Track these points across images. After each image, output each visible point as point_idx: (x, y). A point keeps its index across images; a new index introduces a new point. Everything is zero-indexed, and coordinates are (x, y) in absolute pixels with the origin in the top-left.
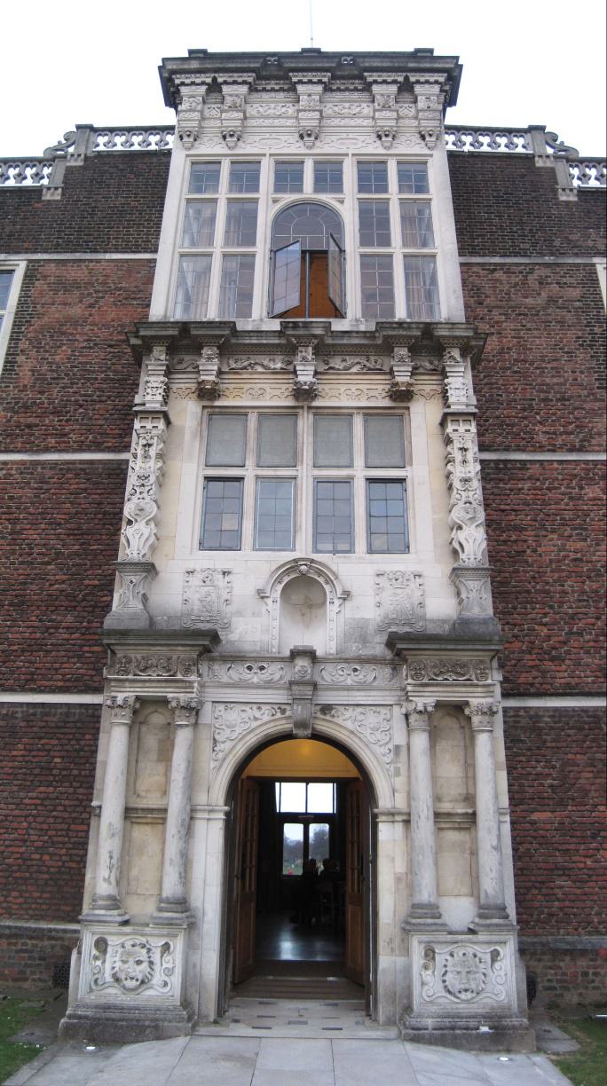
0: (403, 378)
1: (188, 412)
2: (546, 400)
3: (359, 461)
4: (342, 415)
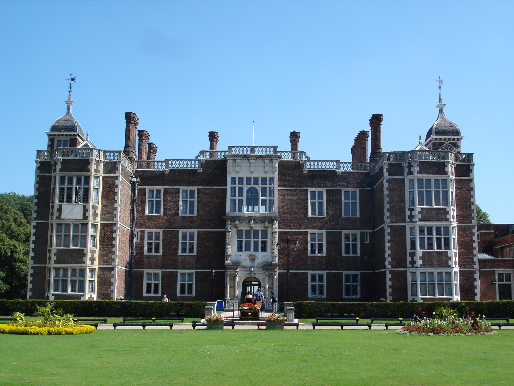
0: (266, 225)
1: (234, 231)
2: (294, 219)
3: (260, 237)
4: (258, 231)
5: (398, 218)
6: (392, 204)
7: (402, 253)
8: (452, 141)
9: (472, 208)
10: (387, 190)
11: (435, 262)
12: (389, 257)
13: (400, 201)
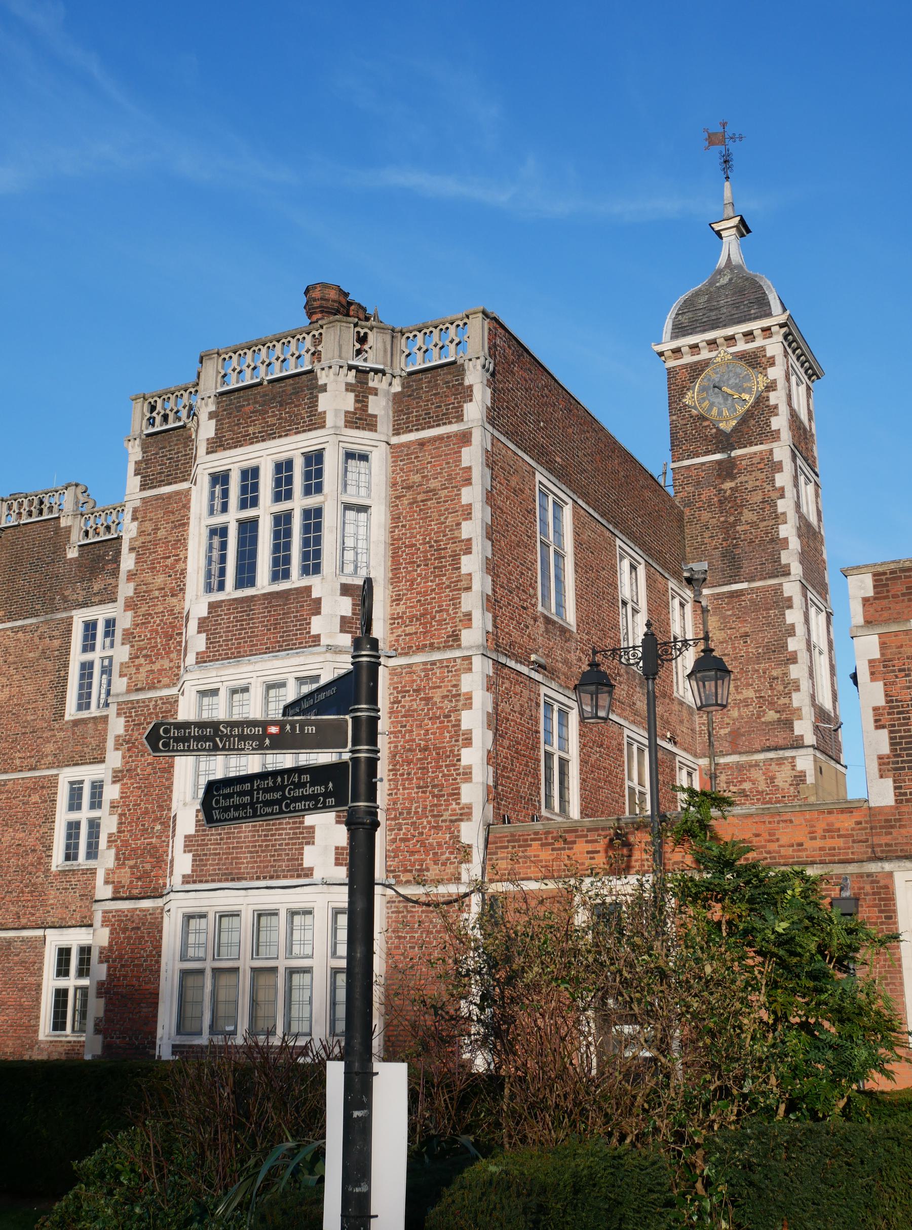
5: (156, 667)
6: (143, 609)
7: (158, 827)
8: (741, 346)
9: (464, 570)
10: (132, 549)
11: (246, 858)
12: (109, 847)
13: (172, 589)
